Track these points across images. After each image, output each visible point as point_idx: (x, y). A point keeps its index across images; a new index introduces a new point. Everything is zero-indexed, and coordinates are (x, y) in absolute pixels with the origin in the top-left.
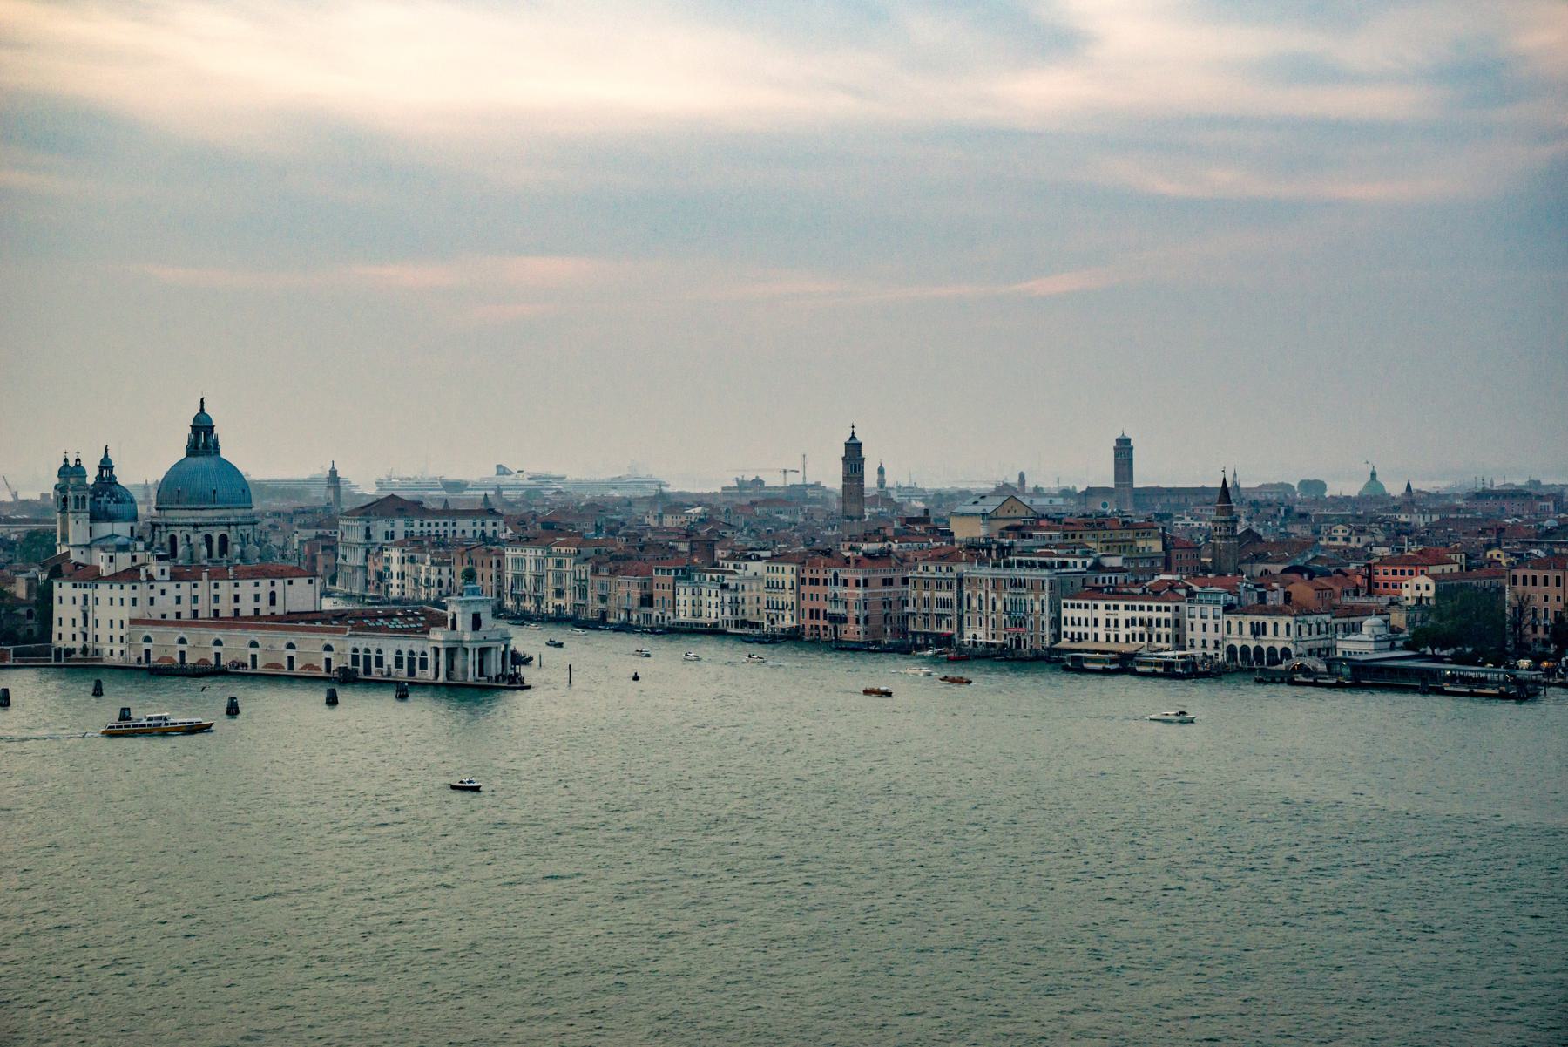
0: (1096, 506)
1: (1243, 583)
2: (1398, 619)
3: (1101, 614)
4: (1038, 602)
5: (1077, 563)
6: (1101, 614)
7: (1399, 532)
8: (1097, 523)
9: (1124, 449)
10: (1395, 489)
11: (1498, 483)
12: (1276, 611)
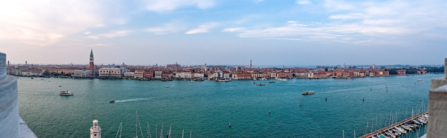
0: (24, 65)
1: (33, 71)
2: (42, 73)
3: (24, 73)
4: (20, 72)
5: (23, 69)
6: (24, 73)
7: (43, 67)
8: (24, 67)
9: (26, 62)
10: (43, 65)
11: (49, 64)
12: (35, 72)
